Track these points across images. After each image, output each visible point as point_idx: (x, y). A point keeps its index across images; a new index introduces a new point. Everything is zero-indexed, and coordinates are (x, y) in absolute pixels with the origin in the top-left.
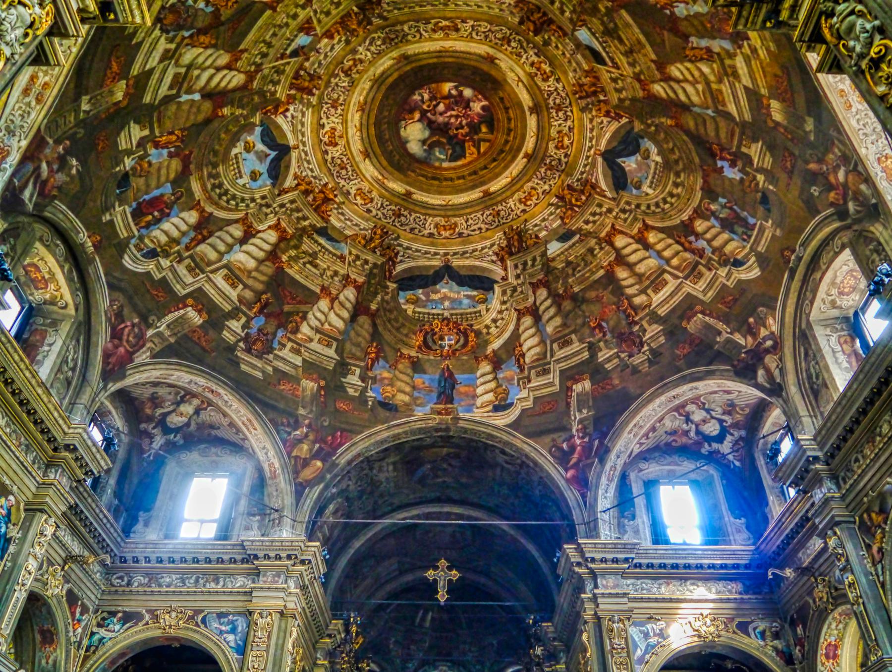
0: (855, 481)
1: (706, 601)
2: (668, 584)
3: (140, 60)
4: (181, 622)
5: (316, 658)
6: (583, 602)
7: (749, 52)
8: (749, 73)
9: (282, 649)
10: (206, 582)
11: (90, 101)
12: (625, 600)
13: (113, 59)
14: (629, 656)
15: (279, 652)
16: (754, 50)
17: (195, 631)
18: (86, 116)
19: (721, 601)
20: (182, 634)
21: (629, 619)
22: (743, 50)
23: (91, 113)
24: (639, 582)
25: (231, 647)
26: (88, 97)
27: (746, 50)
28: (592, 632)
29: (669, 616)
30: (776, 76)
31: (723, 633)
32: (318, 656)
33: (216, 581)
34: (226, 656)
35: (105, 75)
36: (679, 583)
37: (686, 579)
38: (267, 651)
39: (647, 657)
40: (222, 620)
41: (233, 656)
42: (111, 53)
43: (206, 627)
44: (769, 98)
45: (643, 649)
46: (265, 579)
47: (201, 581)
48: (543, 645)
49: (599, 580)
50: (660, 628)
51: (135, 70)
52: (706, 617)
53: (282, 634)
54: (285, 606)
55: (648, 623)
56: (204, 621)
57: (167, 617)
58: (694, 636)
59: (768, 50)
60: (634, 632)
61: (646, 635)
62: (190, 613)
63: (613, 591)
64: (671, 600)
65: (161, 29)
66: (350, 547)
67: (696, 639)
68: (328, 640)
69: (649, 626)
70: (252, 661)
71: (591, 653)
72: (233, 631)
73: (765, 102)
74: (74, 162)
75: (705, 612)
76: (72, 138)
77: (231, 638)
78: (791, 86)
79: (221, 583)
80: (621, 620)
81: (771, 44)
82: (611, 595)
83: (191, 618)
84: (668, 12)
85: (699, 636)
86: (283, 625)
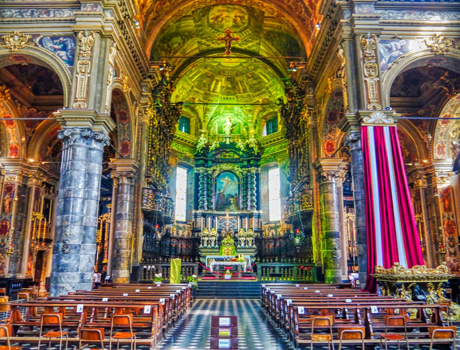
1: (440, 25)
2: (410, 14)
4: (23, 43)
5: (142, 92)
6: (341, 26)
9: (104, 60)
10: (40, 14)
12: (377, 22)
14: (377, 62)
15: (102, 63)
17: (34, 49)
19: (452, 25)
20: (24, 52)
21: (378, 36)
24: (387, 12)
25: (64, 60)
28: (347, 48)
29: (410, 36)
31: (450, 48)
32: (144, 90)
33: (48, 13)
34: (60, 66)
36: (419, 13)
37: (425, 10)
38: (91, 60)
39: (390, 65)
40: (55, 41)
41: (66, 66)
43: (43, 46)
45: (387, 59)
46: (85, 9)
47: (36, 14)
48: (297, 85)
49: (356, 8)
50: (401, 44)
52: (439, 37)
53: (103, 50)
54: (103, 27)
55: (392, 41)
56: (41, 42)
57: (11, 39)
58: (428, 50)
60: (381, 48)
61: (390, 50)
62: (28, 37)
63: (367, 15)
64: (412, 24)
66: (161, 20)
67: (429, 53)
68: (149, 80)
69: (393, 44)
70: (80, 67)
71: (346, 62)
72: (65, 48)
75: (438, 34)
77: (63, 53)
79: (52, 15)
80: (372, 37)
82: (365, 18)
83: (31, 40)
85: (432, 51)
86: (103, 44)
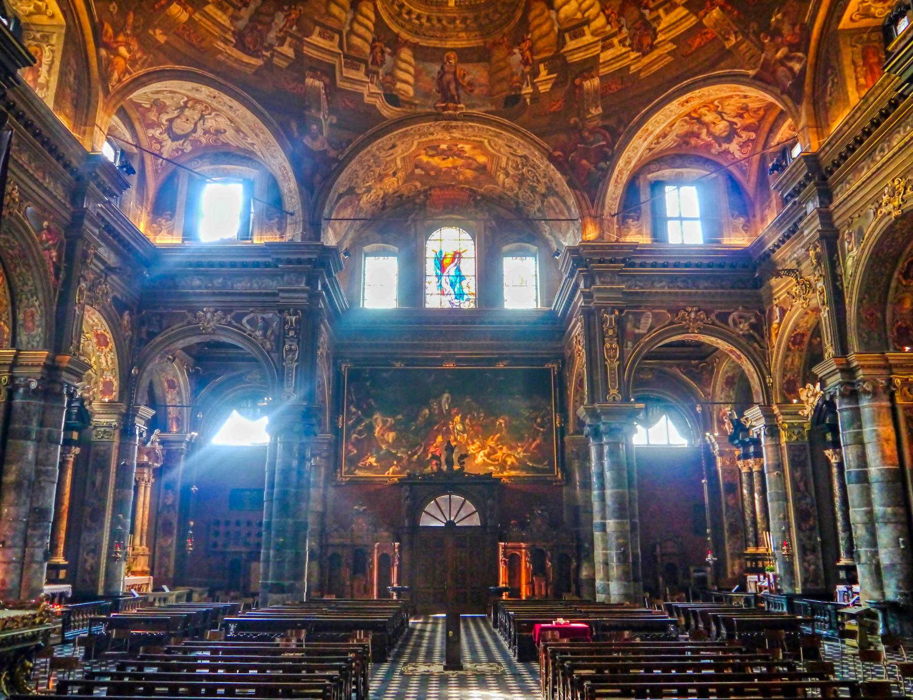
0: (27, 171)
3: (684, 25)
7: (227, 36)
8: (214, 19)
11: (728, 39)
13: (693, 49)
16: (226, 41)
18: (739, 34)
22: (230, 33)
23: (736, 29)
26: (726, 43)
27: (229, 36)
30: (203, 40)
35: (706, 44)
42: (691, 54)
44: (190, 18)
51: (693, 20)
59: (221, 52)
65: (656, 38)
73: (190, 9)
74: (773, 20)
76: (757, 34)
78: (191, 45)
81: (223, 58)
84: (286, 8)
